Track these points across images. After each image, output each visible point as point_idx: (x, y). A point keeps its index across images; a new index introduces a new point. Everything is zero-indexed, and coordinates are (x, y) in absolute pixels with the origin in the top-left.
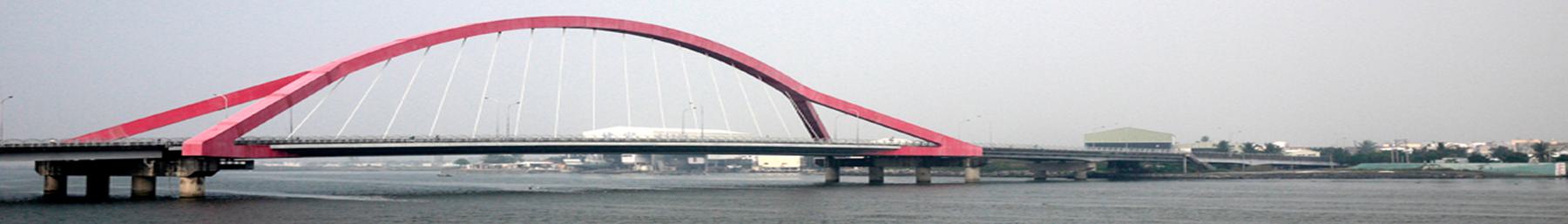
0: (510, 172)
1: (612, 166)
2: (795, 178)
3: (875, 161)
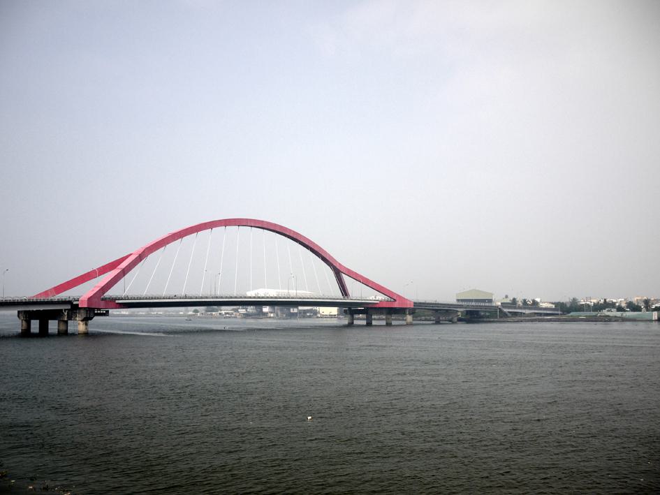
0: (216, 317)
1: (258, 314)
2: (335, 322)
3: (369, 310)
